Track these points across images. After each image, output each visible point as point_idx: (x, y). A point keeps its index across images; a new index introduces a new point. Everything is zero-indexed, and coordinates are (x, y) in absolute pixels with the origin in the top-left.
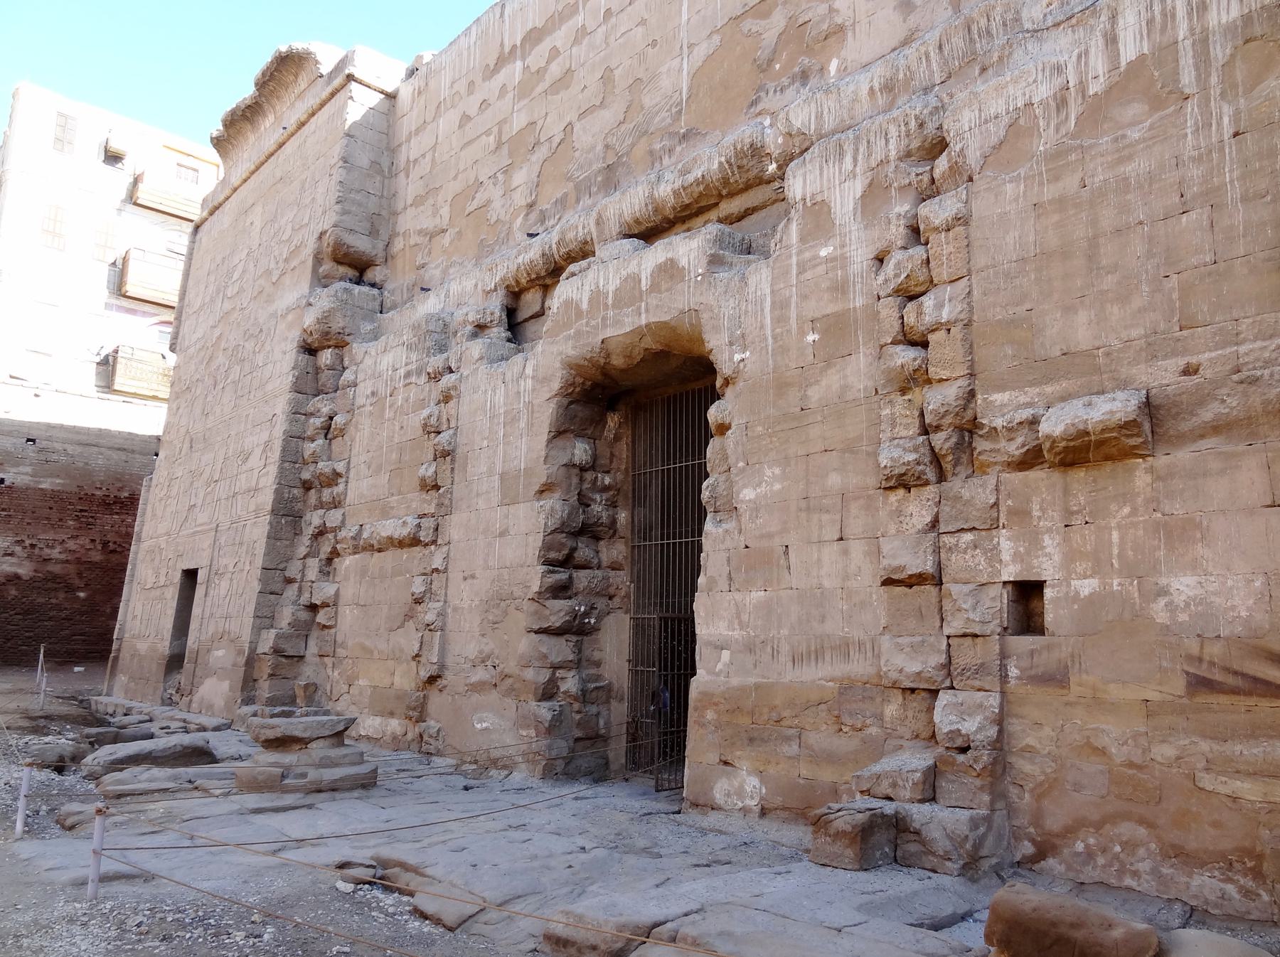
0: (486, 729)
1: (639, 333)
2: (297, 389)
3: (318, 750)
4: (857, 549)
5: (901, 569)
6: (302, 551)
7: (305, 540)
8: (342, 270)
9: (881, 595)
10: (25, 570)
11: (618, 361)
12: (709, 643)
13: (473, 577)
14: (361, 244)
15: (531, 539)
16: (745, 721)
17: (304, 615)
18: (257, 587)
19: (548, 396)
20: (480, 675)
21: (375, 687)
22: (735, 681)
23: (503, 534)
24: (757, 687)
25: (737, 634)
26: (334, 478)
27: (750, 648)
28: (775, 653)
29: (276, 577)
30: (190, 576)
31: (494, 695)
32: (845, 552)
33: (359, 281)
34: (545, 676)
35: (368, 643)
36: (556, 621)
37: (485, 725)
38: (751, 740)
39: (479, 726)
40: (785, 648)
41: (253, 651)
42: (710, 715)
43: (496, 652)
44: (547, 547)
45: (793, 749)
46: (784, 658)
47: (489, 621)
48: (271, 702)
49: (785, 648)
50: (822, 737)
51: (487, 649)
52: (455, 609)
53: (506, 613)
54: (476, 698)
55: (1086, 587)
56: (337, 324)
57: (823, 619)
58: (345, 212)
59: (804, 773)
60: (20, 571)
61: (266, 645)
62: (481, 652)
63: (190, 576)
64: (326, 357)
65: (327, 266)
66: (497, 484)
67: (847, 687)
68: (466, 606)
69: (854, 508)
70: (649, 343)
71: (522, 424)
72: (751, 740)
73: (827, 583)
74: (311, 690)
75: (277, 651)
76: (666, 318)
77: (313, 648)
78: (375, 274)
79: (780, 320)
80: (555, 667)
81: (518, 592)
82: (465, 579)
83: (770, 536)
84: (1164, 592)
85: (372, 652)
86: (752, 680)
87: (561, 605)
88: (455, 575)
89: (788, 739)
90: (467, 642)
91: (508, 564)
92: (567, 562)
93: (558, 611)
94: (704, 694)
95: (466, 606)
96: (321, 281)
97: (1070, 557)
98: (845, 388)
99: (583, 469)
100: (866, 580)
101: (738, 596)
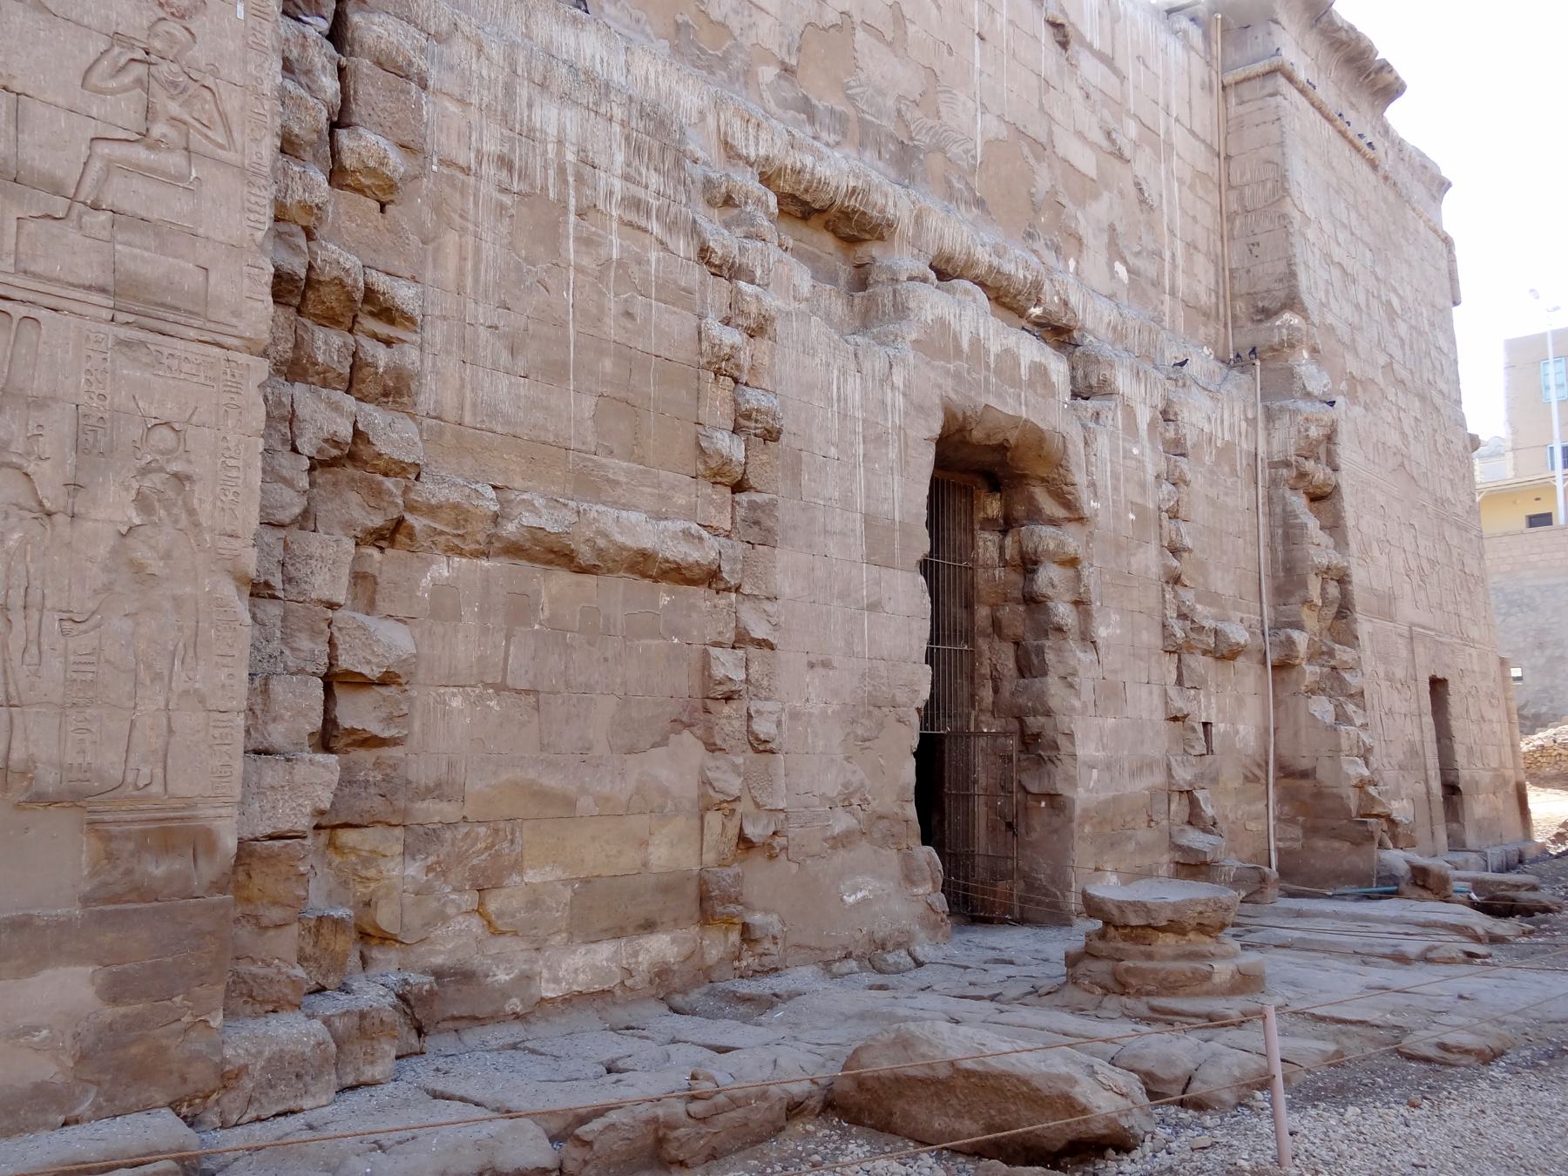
0: (864, 899)
1: (1016, 421)
4: (1156, 690)
5: (1181, 710)
9: (1164, 726)
11: (977, 435)
12: (1085, 763)
13: (826, 664)
15: (915, 625)
16: (1107, 829)
19: (927, 435)
20: (842, 822)
21: (586, 881)
22: (1103, 796)
23: (874, 607)
24: (1115, 798)
25: (1101, 754)
27: (1109, 767)
28: (1122, 769)
31: (864, 849)
32: (1151, 693)
35: (552, 781)
37: (859, 895)
38: (1112, 845)
39: (851, 900)
40: (1126, 766)
42: (1087, 829)
43: (867, 782)
45: (1131, 846)
46: (1126, 775)
47: (856, 737)
49: (1126, 766)
50: (1144, 834)
51: (855, 780)
52: (795, 716)
53: (881, 726)
54: (842, 856)
55: (1222, 727)
57: (1142, 742)
59: (1138, 863)
62: (845, 786)
66: (859, 526)
67: (1154, 792)
68: (816, 711)
69: (1154, 659)
70: (1013, 437)
71: (893, 453)
72: (1112, 845)
73: (1145, 715)
76: (1041, 425)
79: (1116, 489)
81: (901, 697)
82: (812, 666)
83: (1114, 672)
84: (1237, 732)
85: (570, 803)
86: (1111, 794)
88: (790, 659)
89: (1130, 838)
91: (885, 654)
94: (1085, 810)
95: (816, 711)
97: (1220, 710)
98: (1147, 568)
100: (1159, 715)
101: (1100, 720)
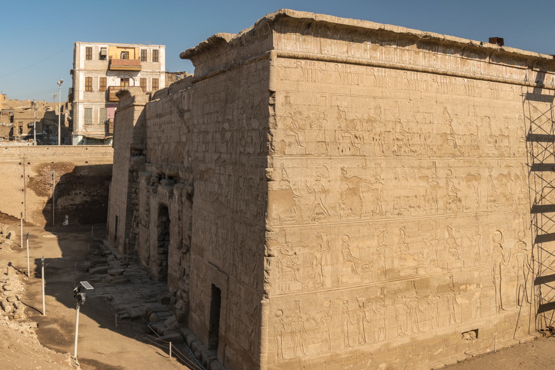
2: (129, 181)
3: (117, 276)
6: (133, 220)
7: (133, 217)
8: (136, 152)
10: (88, 199)
14: (139, 146)
17: (134, 235)
18: (125, 228)
26: (137, 205)
29: (128, 226)
30: (117, 217)
33: (140, 155)
34: (160, 262)
36: (161, 252)
41: (125, 242)
44: (158, 238)
48: (129, 254)
56: (135, 167)
58: (135, 140)
60: (88, 200)
61: (127, 242)
63: (117, 217)
64: (135, 173)
65: (133, 151)
74: (137, 252)
75: (129, 243)
77: (136, 243)
78: (144, 152)
80: (162, 261)
87: (162, 249)
90: (152, 253)
92: (164, 240)
93: (161, 250)
96: (133, 155)
99: (165, 222)
